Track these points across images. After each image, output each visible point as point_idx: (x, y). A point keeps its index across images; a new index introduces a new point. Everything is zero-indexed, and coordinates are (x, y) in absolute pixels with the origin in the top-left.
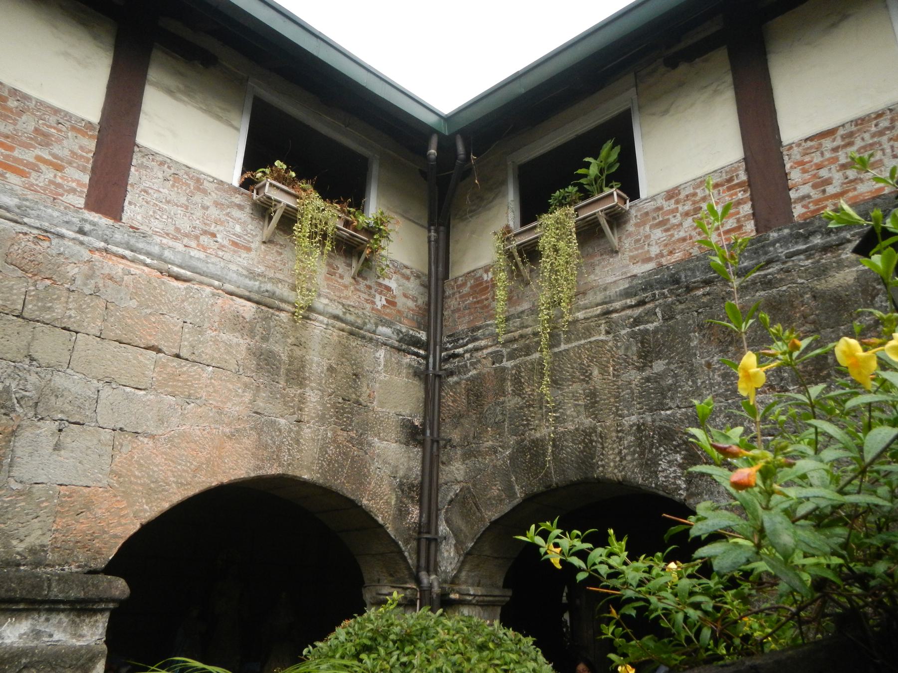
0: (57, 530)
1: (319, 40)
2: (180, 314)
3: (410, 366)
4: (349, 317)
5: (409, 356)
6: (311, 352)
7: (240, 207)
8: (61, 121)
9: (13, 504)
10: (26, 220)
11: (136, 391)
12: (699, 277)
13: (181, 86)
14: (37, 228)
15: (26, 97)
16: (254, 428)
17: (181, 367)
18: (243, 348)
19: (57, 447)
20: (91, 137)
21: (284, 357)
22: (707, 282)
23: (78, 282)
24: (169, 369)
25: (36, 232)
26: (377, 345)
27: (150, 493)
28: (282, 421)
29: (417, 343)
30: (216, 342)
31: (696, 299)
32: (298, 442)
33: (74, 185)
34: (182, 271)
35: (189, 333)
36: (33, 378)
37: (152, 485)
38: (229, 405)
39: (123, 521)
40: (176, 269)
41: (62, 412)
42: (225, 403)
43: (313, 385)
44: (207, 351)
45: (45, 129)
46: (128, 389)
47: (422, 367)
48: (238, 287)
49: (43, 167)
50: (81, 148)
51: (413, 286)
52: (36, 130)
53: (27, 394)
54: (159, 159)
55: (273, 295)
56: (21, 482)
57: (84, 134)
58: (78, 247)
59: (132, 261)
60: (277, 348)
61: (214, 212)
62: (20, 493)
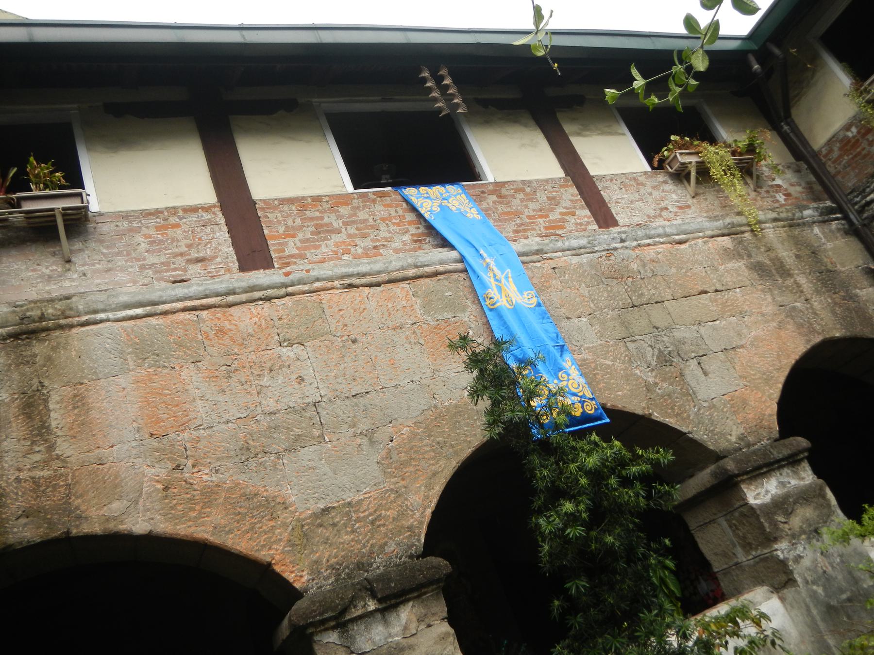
0: (741, 423)
1: (652, 38)
2: (699, 264)
3: (839, 230)
4: (783, 215)
5: (833, 223)
6: (779, 251)
7: (665, 182)
8: (553, 185)
9: (711, 415)
10: (596, 249)
11: (715, 322)
13: (580, 127)
14: (603, 251)
15: (530, 182)
16: (787, 317)
17: (724, 296)
18: (743, 268)
19: (706, 374)
20: (571, 186)
23: (642, 272)
24: (719, 301)
25: (604, 253)
26: (810, 226)
27: (768, 380)
28: (798, 304)
29: (831, 211)
30: (727, 271)
32: (817, 315)
33: (586, 219)
34: (681, 237)
35: (711, 273)
37: (765, 377)
38: (764, 308)
39: (767, 405)
40: (677, 237)
41: (693, 352)
42: (760, 308)
43: (796, 272)
44: (728, 279)
45: (550, 195)
46: (710, 323)
47: (846, 226)
48: (713, 230)
49: (566, 217)
50: (572, 195)
51: (789, 175)
52: (548, 198)
53: (669, 349)
54: (608, 178)
55: (733, 225)
56: (706, 401)
57: (568, 186)
58: (627, 251)
59: (654, 245)
60: (760, 258)
61: (656, 194)
62: (710, 408)
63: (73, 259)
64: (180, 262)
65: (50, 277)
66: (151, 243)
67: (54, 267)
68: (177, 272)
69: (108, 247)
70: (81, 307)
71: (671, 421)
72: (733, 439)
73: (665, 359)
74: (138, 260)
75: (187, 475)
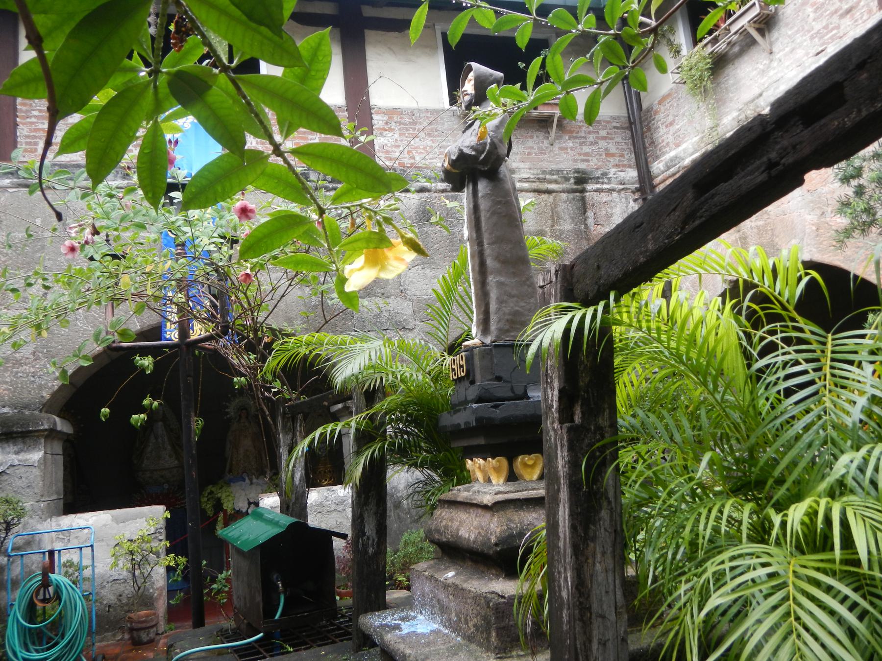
63: (774, 50)
64: (835, 19)
65: (763, 71)
66: (815, 11)
67: (765, 62)
68: (834, 32)
69: (792, 28)
70: (762, 104)
74: (809, 31)
75: (828, 219)
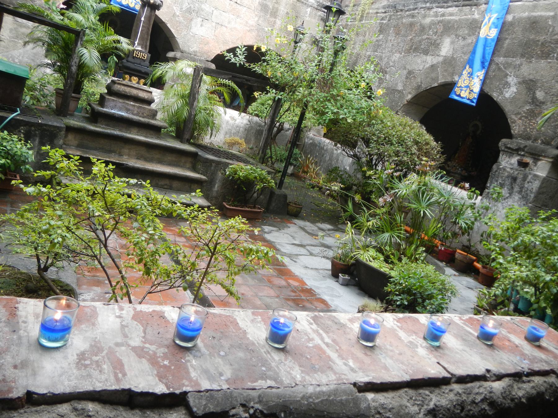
3: (320, 16)
12: (401, 8)
19: (202, 25)
21: (271, 7)
22: (401, 10)
31: (397, 15)
36: (197, 5)
62: (192, 36)
71: (173, 31)
72: (192, 50)
73: (189, 11)
